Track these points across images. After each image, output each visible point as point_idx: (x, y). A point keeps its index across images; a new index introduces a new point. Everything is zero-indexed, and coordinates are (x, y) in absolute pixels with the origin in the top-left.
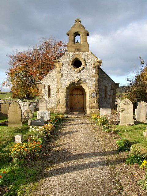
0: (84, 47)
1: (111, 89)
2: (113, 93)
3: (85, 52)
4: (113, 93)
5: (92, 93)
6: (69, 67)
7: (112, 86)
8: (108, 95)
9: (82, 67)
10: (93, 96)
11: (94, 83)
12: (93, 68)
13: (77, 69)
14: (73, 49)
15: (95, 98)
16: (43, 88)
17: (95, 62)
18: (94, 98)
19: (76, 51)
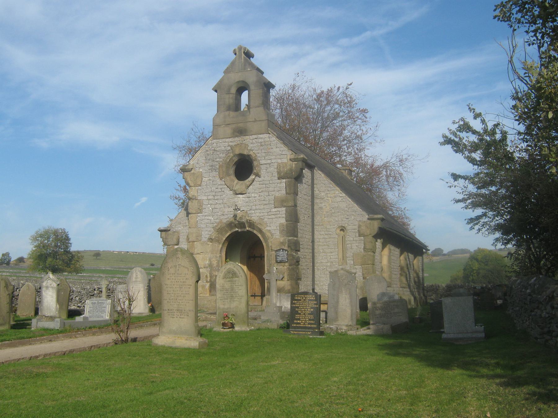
0: (255, 121)
1: (357, 235)
2: (363, 247)
3: (259, 136)
4: (364, 248)
5: (276, 251)
6: (219, 182)
7: (359, 226)
8: (349, 254)
9: (252, 177)
10: (279, 259)
11: (283, 221)
12: (279, 179)
13: (239, 185)
14: (229, 130)
15: (287, 264)
16: (175, 241)
17: (285, 161)
18: (283, 264)
19: (237, 136)
